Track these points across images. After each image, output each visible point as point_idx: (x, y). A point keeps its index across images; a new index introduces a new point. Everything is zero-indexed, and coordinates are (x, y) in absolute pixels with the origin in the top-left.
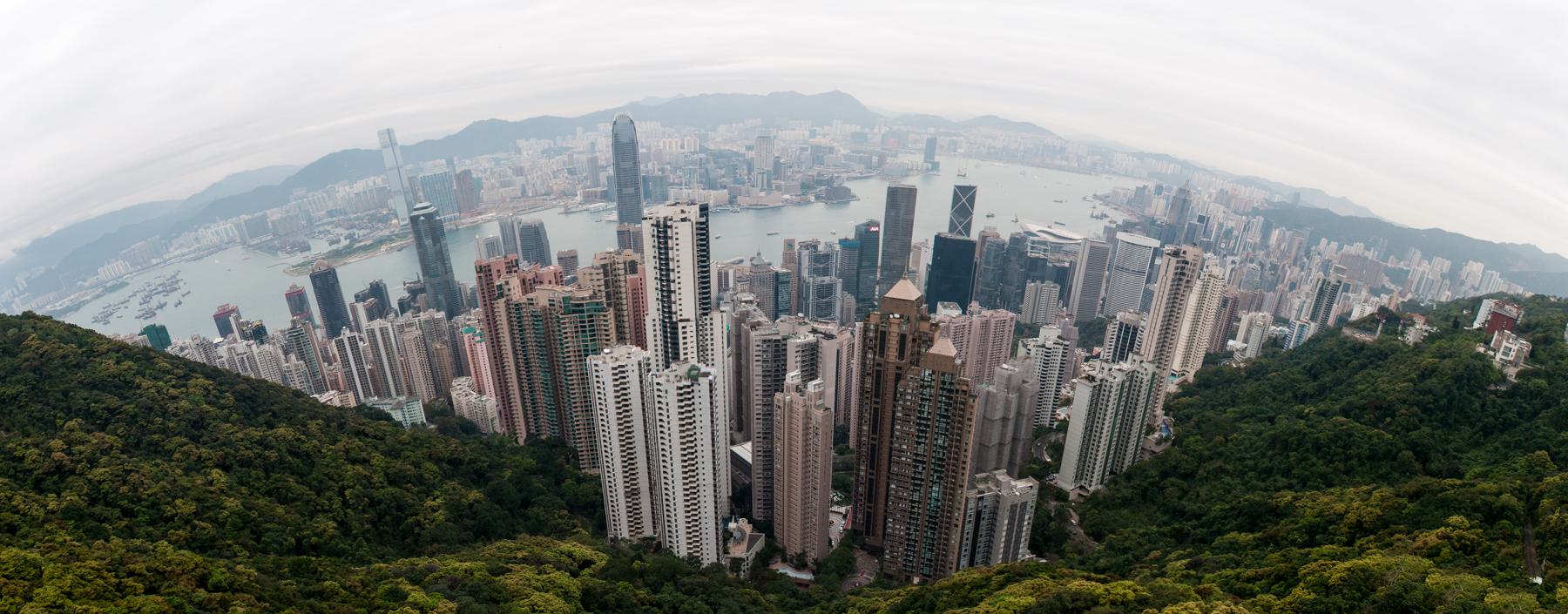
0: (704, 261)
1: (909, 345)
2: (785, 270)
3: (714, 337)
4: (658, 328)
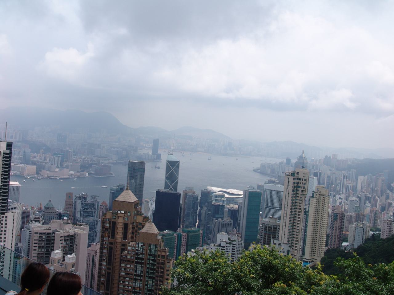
0: (6, 179)
1: (130, 231)
2: (65, 212)
3: (7, 229)
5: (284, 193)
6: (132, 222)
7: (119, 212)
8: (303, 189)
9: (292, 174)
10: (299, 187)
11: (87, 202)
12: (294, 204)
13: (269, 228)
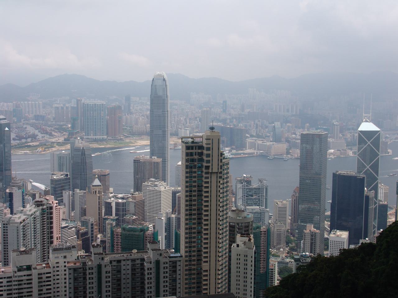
11: (251, 187)
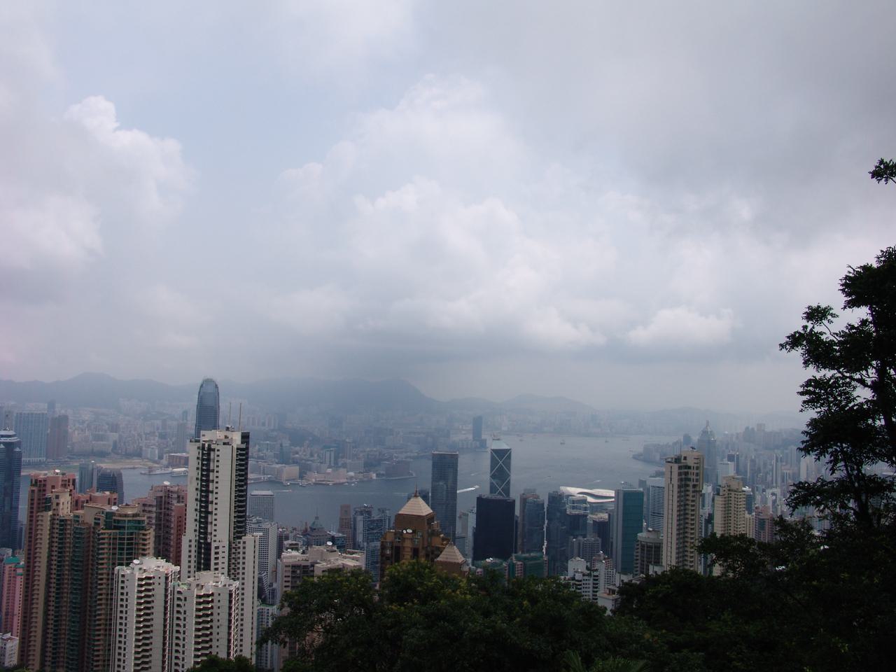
0: (242, 486)
2: (340, 535)
3: (246, 561)
4: (193, 549)
5: (666, 490)
6: (426, 546)
7: (405, 532)
8: (695, 483)
9: (677, 460)
10: (689, 480)
11: (372, 519)
12: (682, 508)
13: (647, 547)
